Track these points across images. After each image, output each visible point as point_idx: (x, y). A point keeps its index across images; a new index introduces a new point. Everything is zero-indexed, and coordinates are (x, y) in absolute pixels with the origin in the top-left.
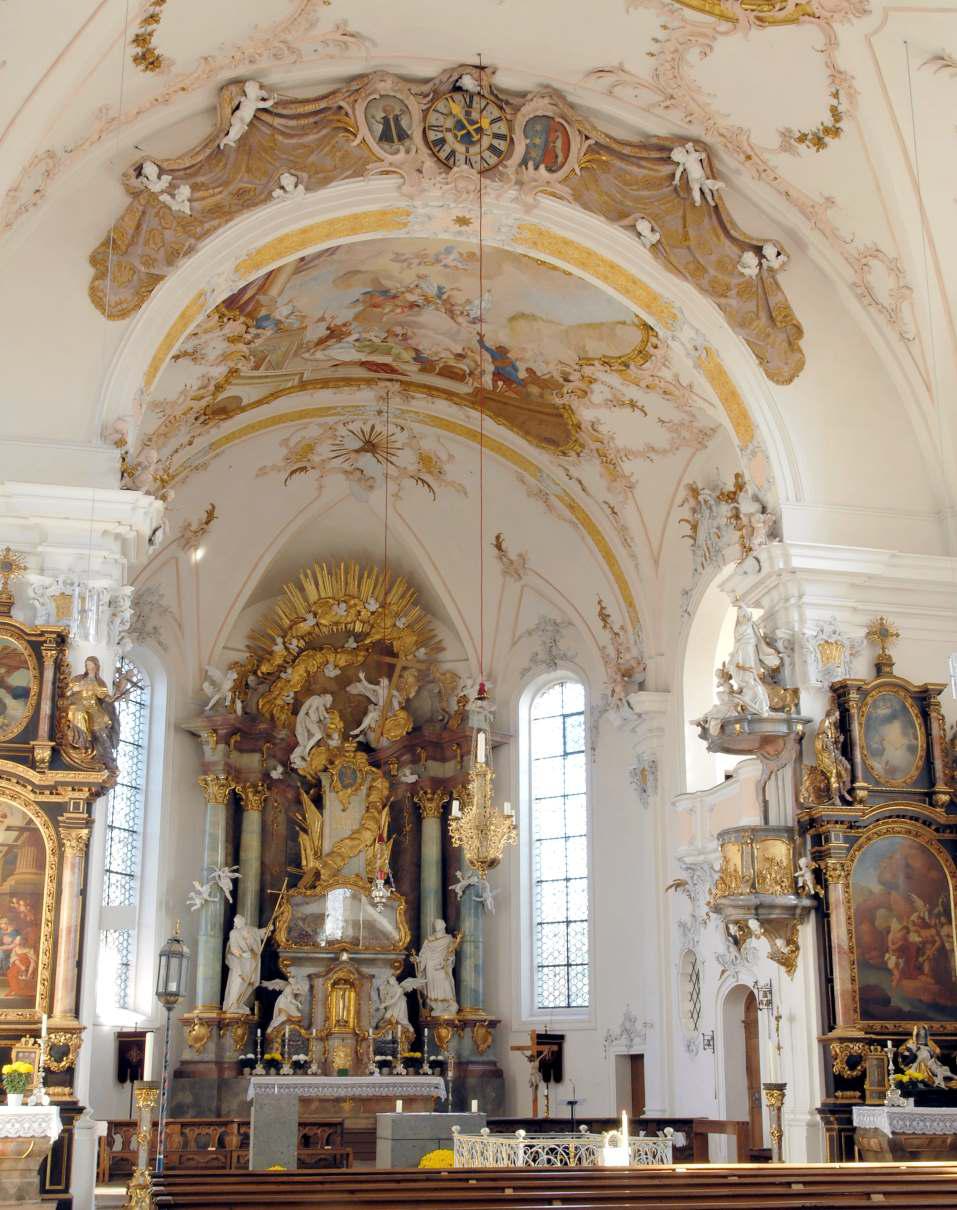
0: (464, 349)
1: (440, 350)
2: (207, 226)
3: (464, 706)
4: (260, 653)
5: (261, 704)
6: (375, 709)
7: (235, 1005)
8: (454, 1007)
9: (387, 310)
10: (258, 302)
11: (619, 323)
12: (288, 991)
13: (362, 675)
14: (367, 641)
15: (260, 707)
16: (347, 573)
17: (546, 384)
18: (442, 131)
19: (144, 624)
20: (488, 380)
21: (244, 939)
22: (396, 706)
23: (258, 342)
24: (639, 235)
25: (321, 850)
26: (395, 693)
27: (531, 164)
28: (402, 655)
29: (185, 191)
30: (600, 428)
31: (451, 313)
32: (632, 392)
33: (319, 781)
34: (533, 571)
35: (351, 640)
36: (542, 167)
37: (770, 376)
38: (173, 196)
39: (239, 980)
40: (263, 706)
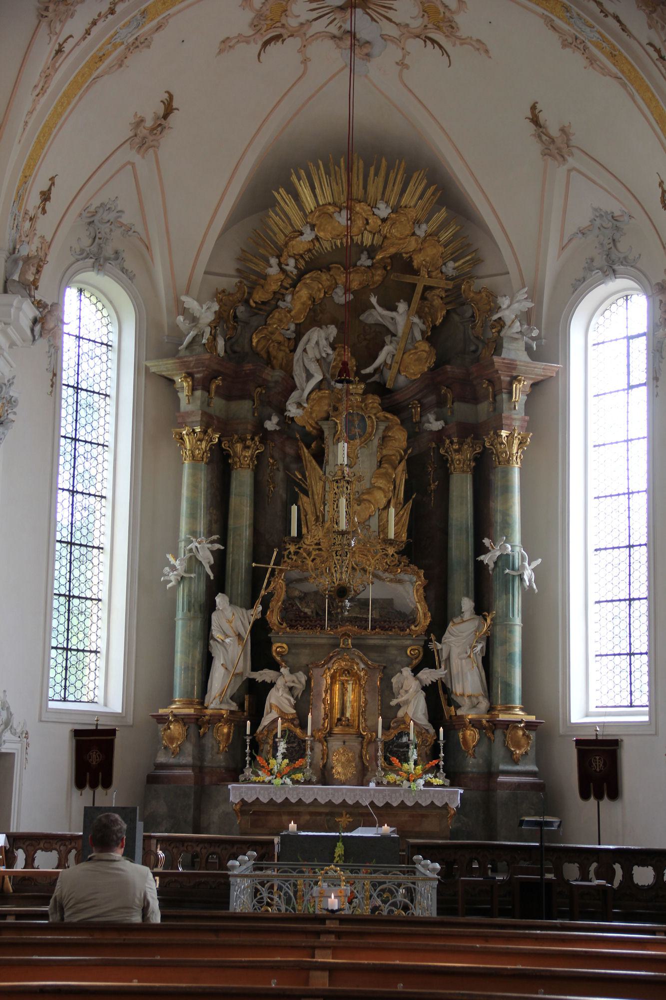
3: (499, 332)
4: (254, 277)
5: (255, 341)
6: (391, 342)
7: (217, 700)
8: (484, 704)
12: (280, 682)
13: (374, 300)
14: (379, 257)
15: (254, 344)
16: (349, 169)
19: (100, 247)
21: (230, 622)
22: (418, 336)
25: (323, 516)
26: (416, 320)
28: (424, 272)
33: (321, 432)
34: (578, 148)
35: (364, 256)
39: (222, 670)
40: (258, 341)
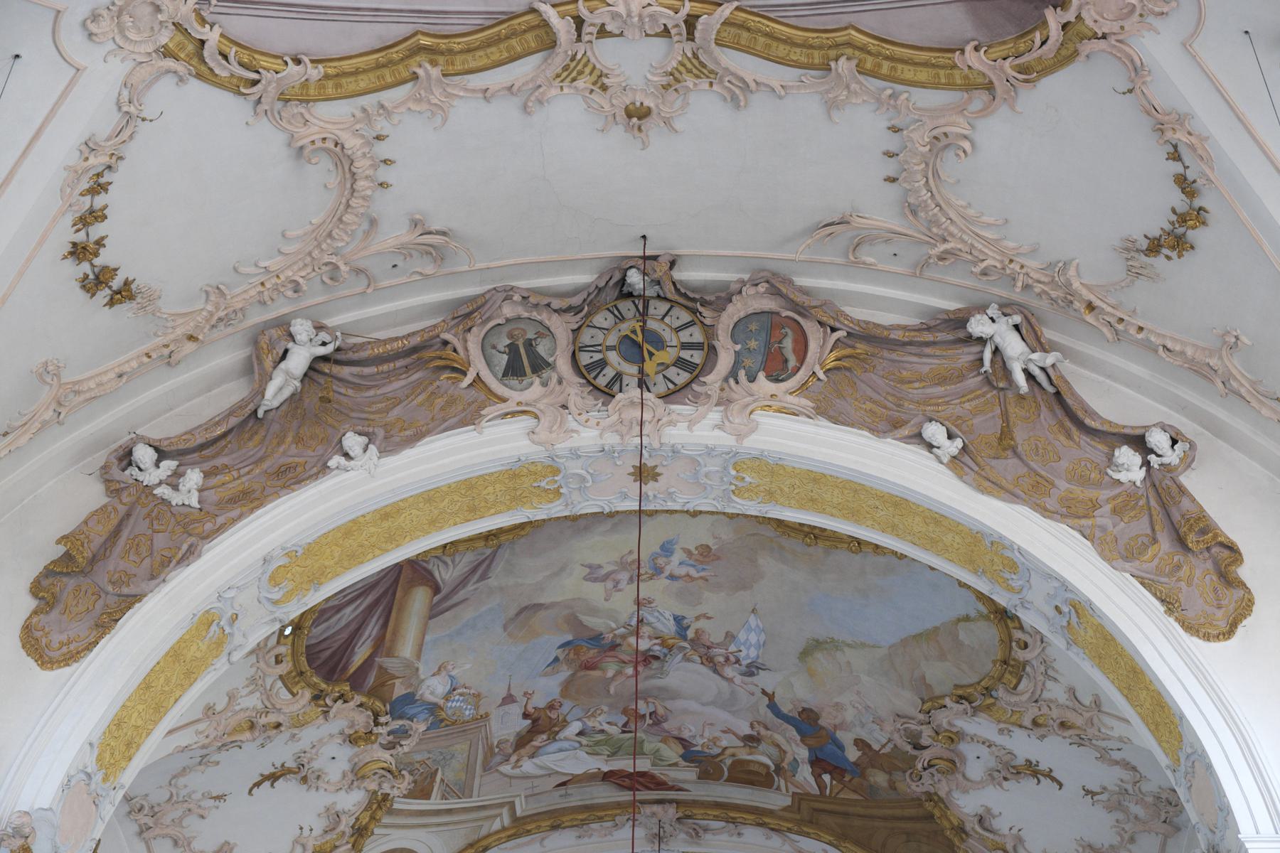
0: (752, 726)
1: (718, 734)
2: (220, 520)
9: (610, 674)
10: (383, 670)
11: (959, 620)
17: (896, 762)
18: (600, 351)
20: (805, 774)
23: (407, 745)
24: (930, 447)
27: (742, 374)
29: (194, 477)
30: (996, 824)
31: (709, 661)
32: (1024, 746)
36: (761, 375)
37: (1189, 628)
38: (175, 488)
